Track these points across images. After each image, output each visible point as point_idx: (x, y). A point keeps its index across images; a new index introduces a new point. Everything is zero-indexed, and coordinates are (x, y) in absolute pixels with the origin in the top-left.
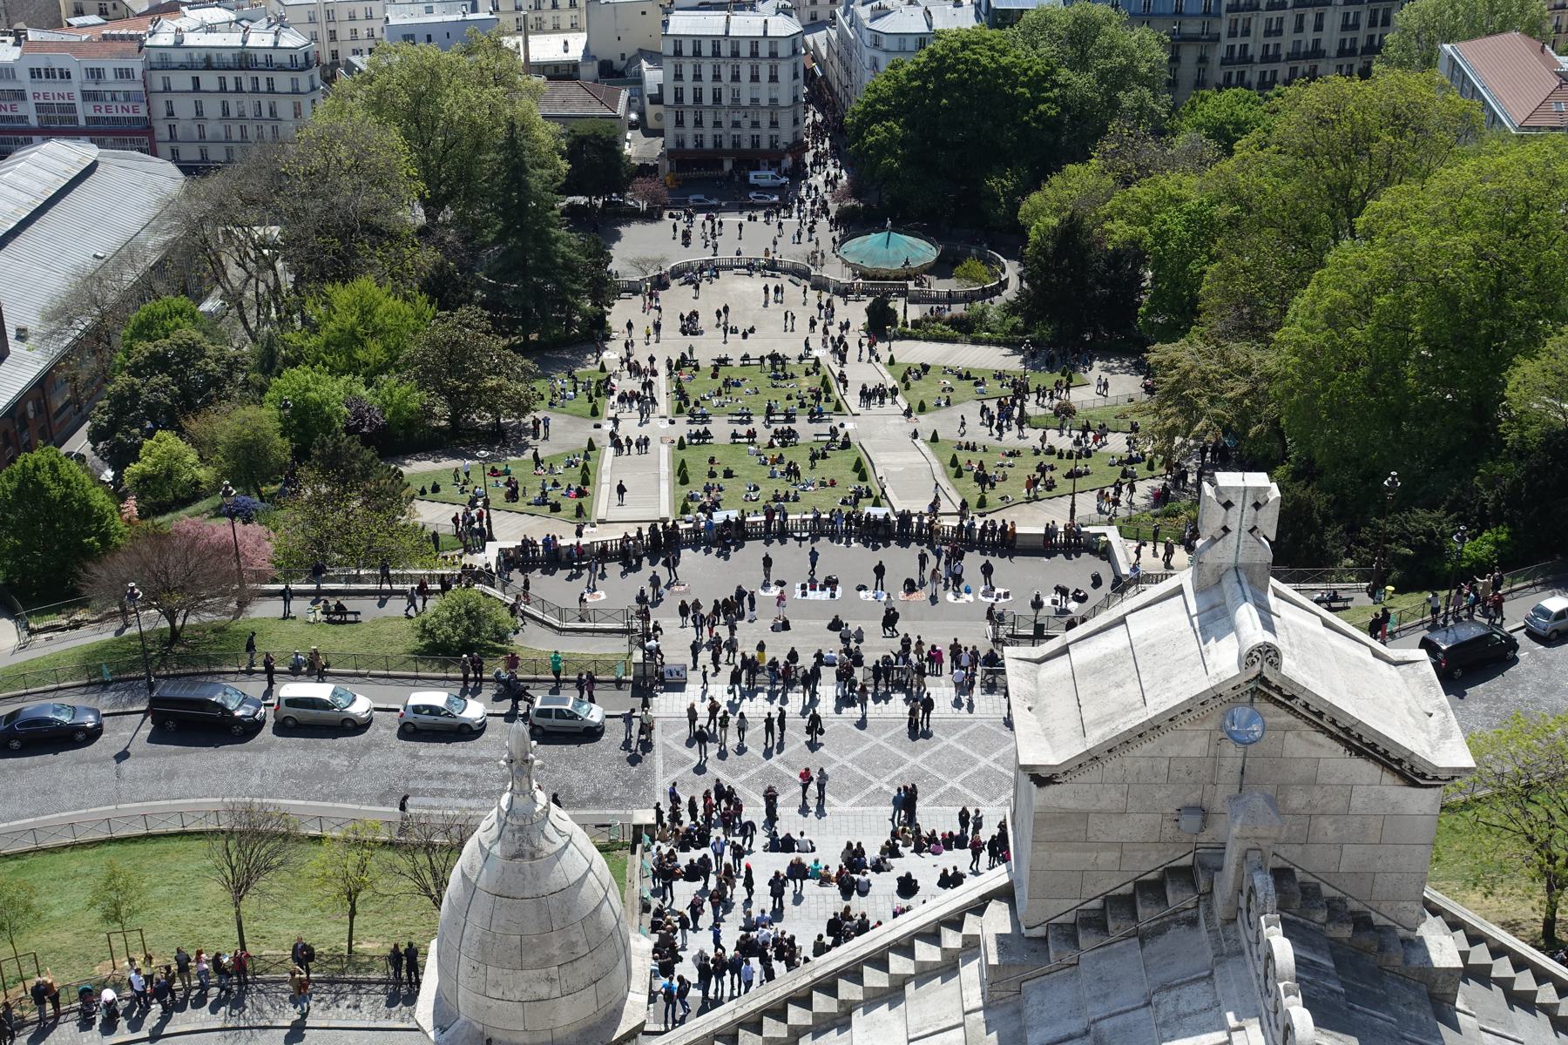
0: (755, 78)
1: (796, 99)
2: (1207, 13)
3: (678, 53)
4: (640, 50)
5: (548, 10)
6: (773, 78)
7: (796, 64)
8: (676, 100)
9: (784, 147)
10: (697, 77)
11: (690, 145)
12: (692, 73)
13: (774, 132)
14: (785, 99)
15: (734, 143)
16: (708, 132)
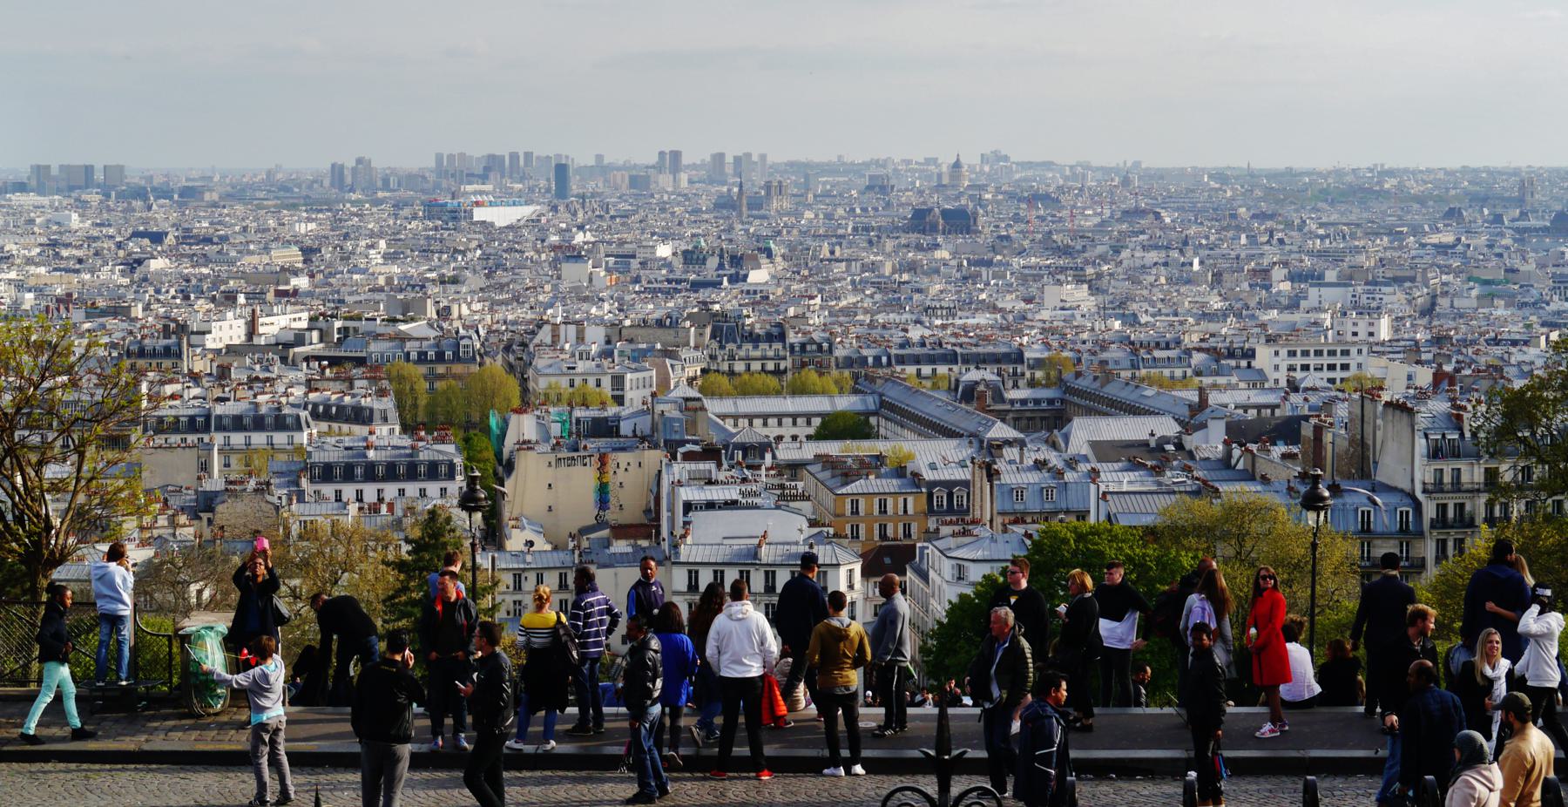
2: (1404, 530)
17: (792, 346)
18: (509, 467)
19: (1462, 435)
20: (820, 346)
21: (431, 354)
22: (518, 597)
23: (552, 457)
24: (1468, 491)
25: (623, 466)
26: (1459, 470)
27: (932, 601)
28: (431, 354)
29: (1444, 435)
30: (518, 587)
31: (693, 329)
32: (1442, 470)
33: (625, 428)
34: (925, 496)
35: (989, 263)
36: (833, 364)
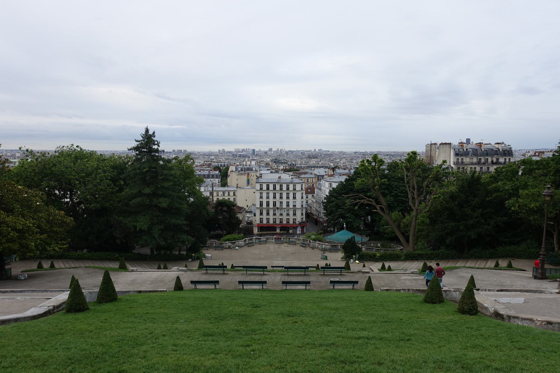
0: (288, 198)
1: (302, 206)
3: (261, 189)
4: (253, 204)
5: (226, 196)
6: (294, 198)
7: (302, 193)
8: (260, 206)
9: (298, 223)
10: (268, 197)
11: (265, 222)
12: (266, 196)
13: (295, 217)
14: (298, 206)
15: (280, 222)
16: (271, 217)
17: (289, 164)
18: (229, 175)
19: (463, 150)
20: (294, 164)
21: (223, 165)
22: (223, 197)
23: (238, 174)
24: (465, 164)
25: (253, 175)
26: (463, 159)
27: (322, 194)
28: (223, 165)
29: (459, 150)
30: (224, 195)
31: (271, 162)
32: (458, 159)
33: (254, 169)
34: (317, 178)
35: (320, 162)
36: (296, 168)
